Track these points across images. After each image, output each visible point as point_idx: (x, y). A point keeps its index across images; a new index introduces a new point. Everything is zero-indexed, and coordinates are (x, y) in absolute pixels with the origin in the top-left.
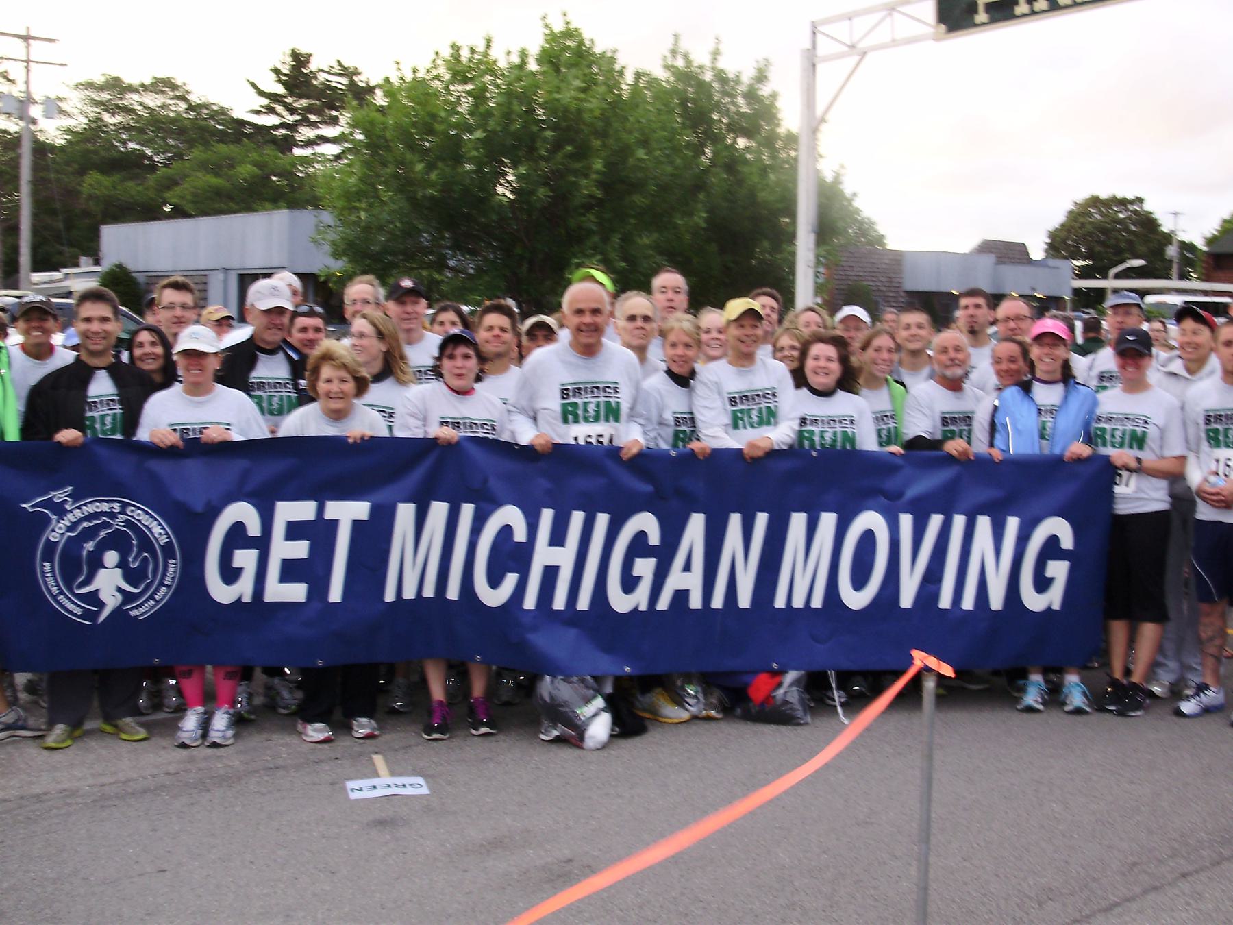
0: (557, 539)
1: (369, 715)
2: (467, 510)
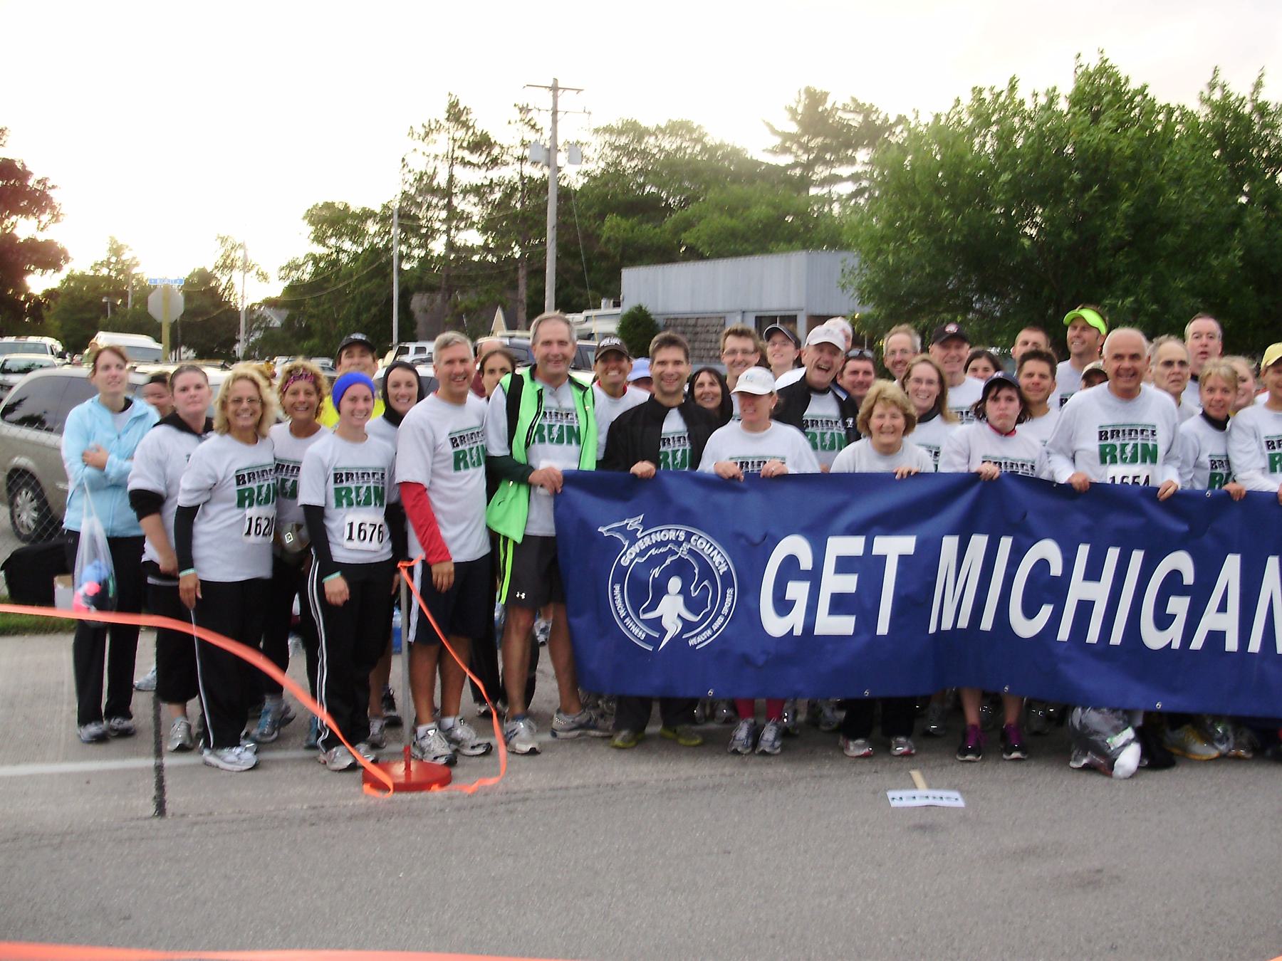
0: (1093, 573)
1: (907, 733)
2: (1006, 543)
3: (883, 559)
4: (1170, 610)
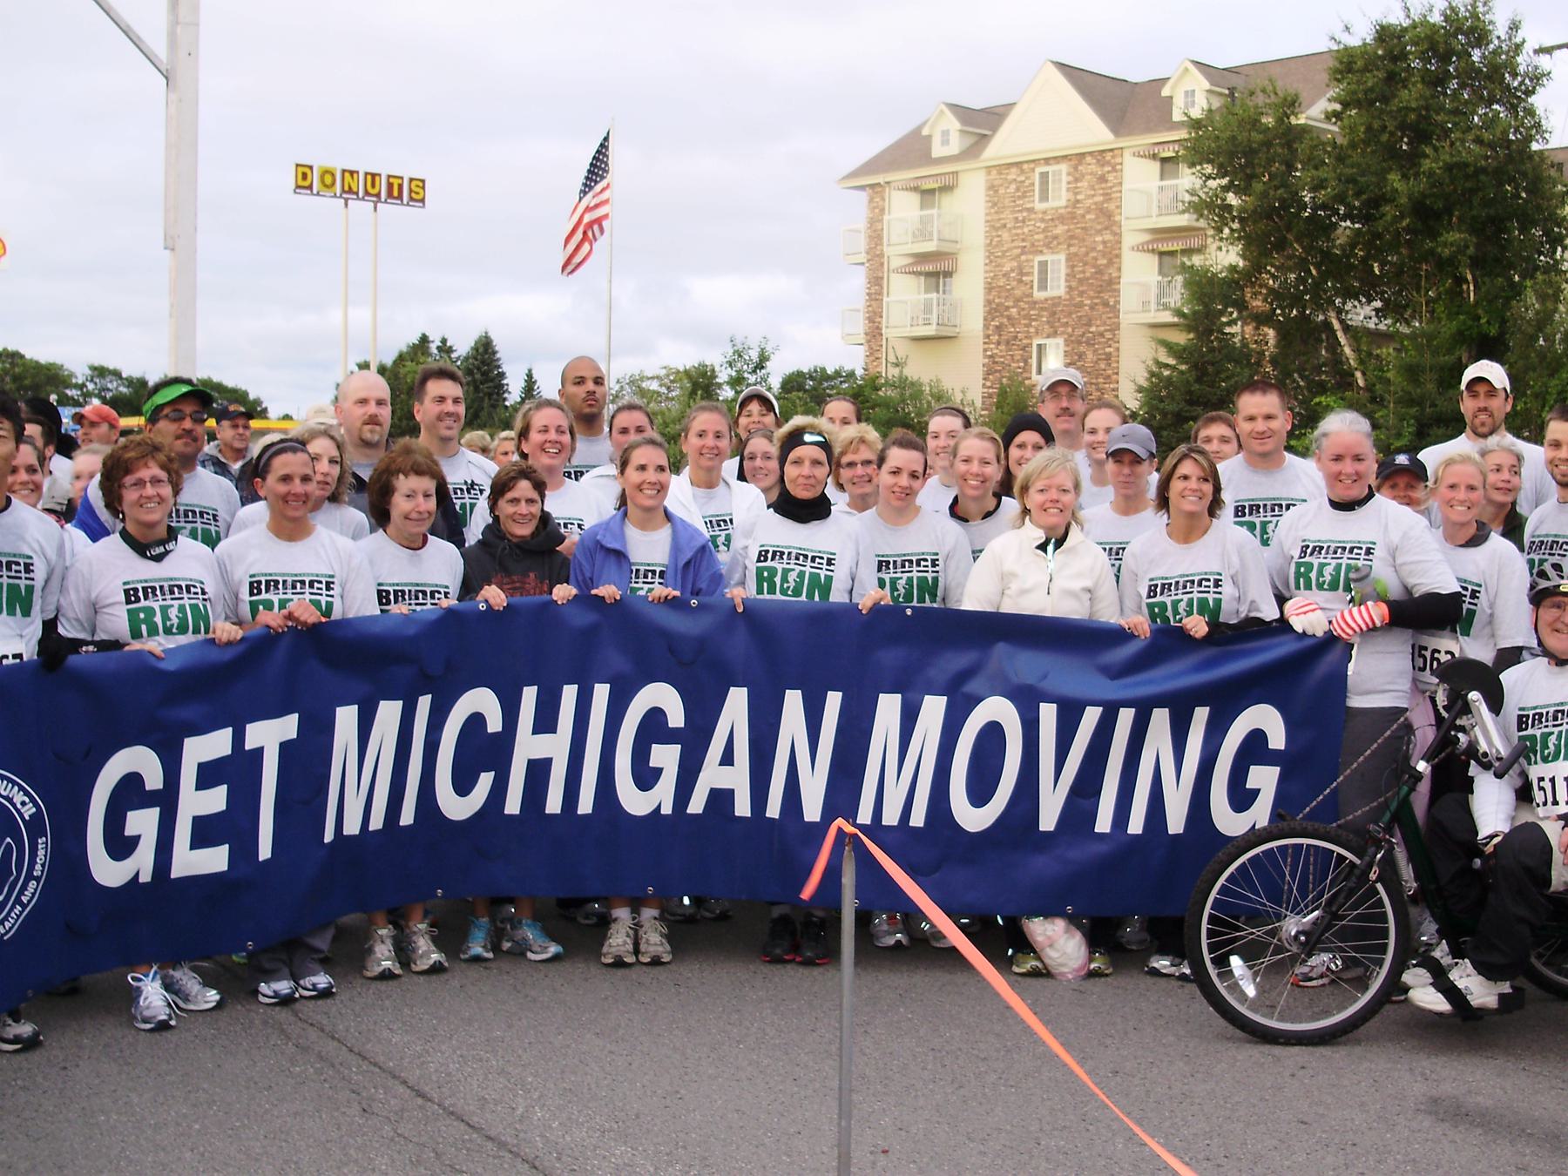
3: (259, 752)
4: (654, 762)
